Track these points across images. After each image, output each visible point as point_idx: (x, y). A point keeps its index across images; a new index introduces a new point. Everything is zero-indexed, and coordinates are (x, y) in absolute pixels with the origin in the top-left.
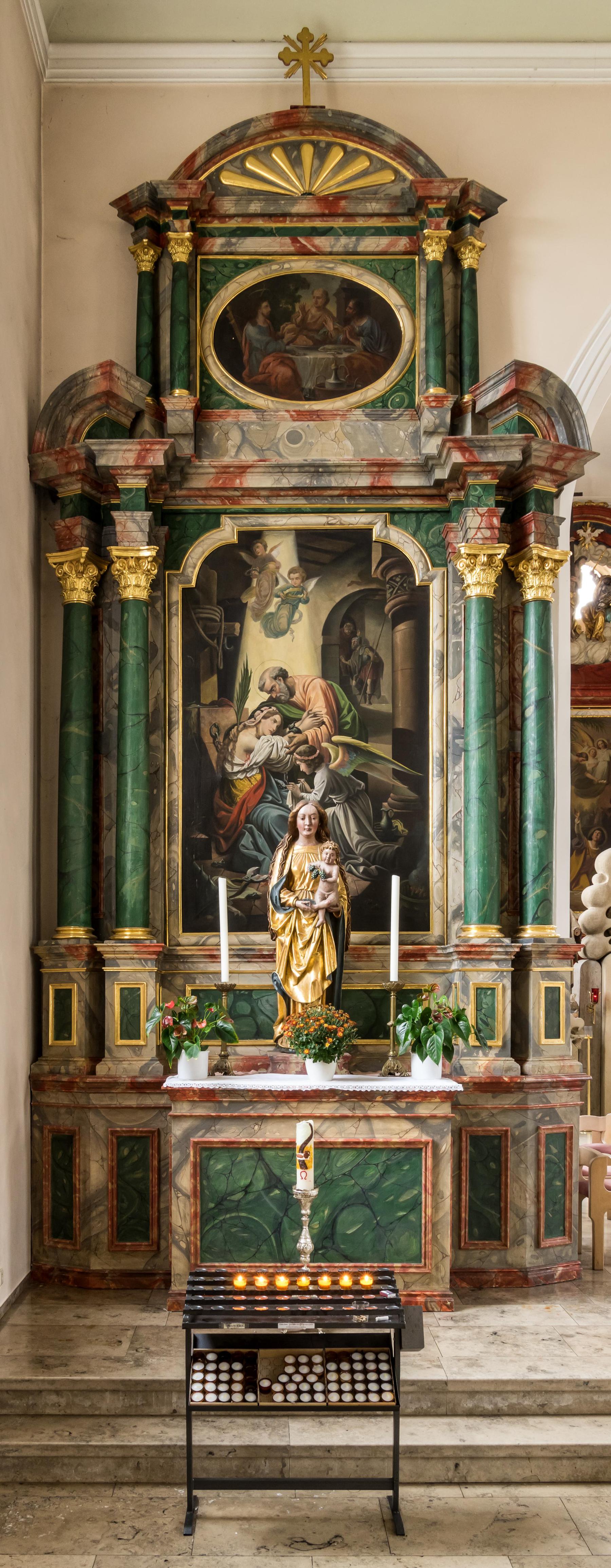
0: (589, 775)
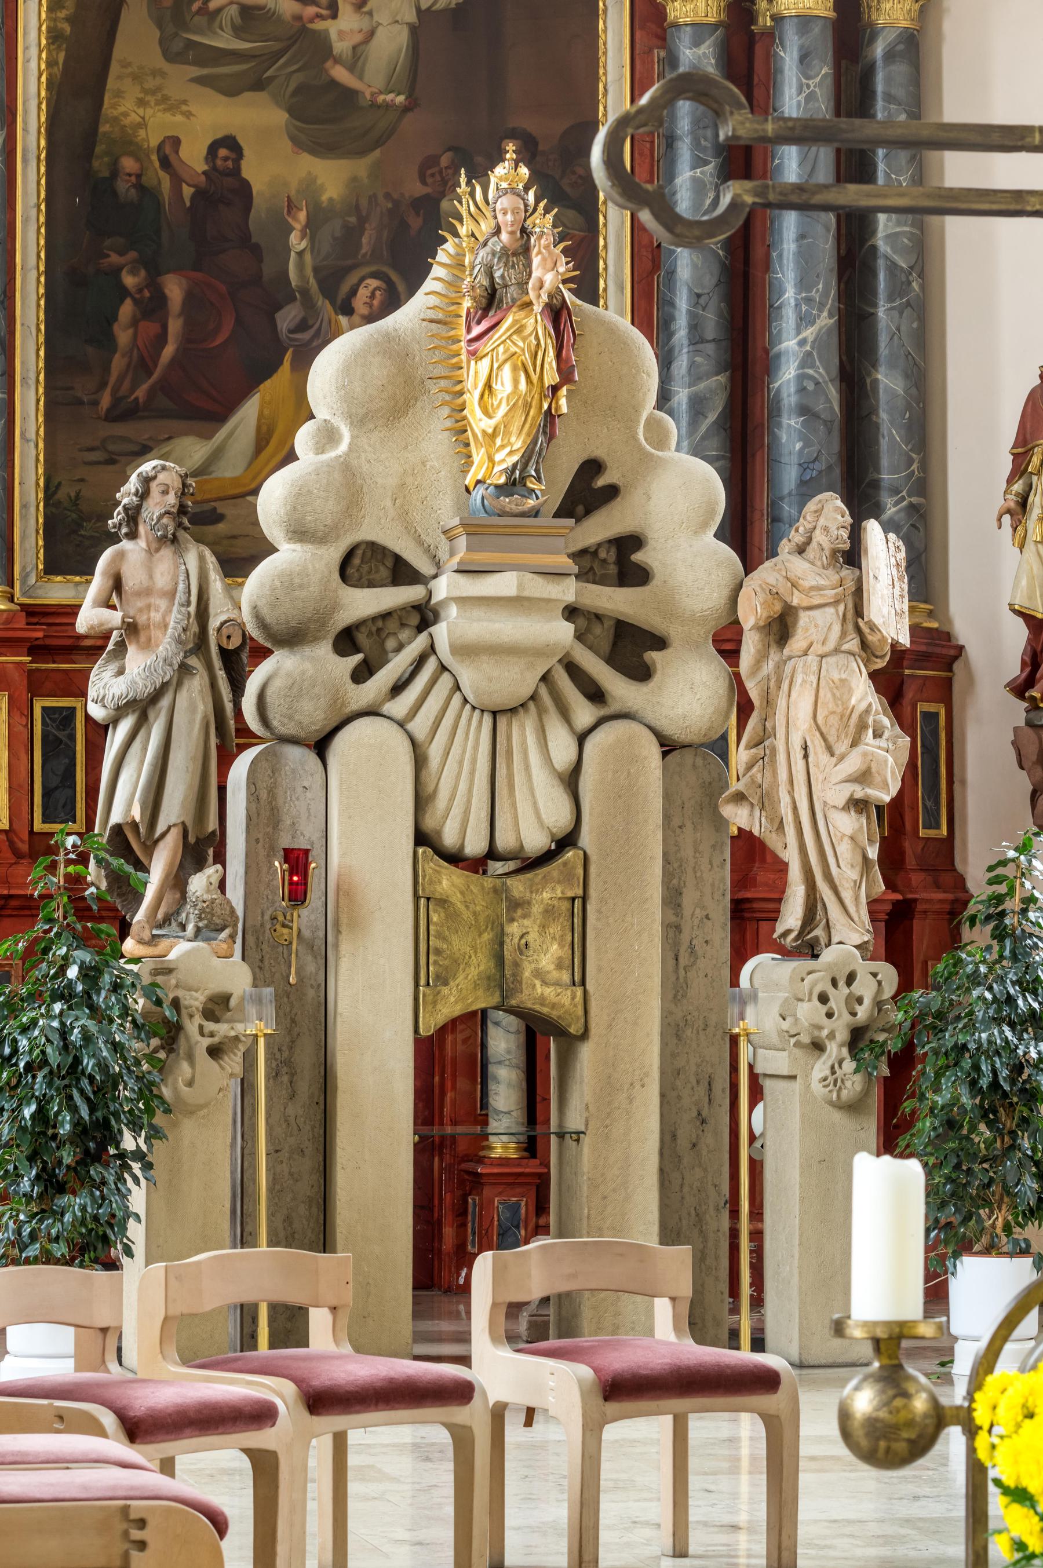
0: (340, 74)
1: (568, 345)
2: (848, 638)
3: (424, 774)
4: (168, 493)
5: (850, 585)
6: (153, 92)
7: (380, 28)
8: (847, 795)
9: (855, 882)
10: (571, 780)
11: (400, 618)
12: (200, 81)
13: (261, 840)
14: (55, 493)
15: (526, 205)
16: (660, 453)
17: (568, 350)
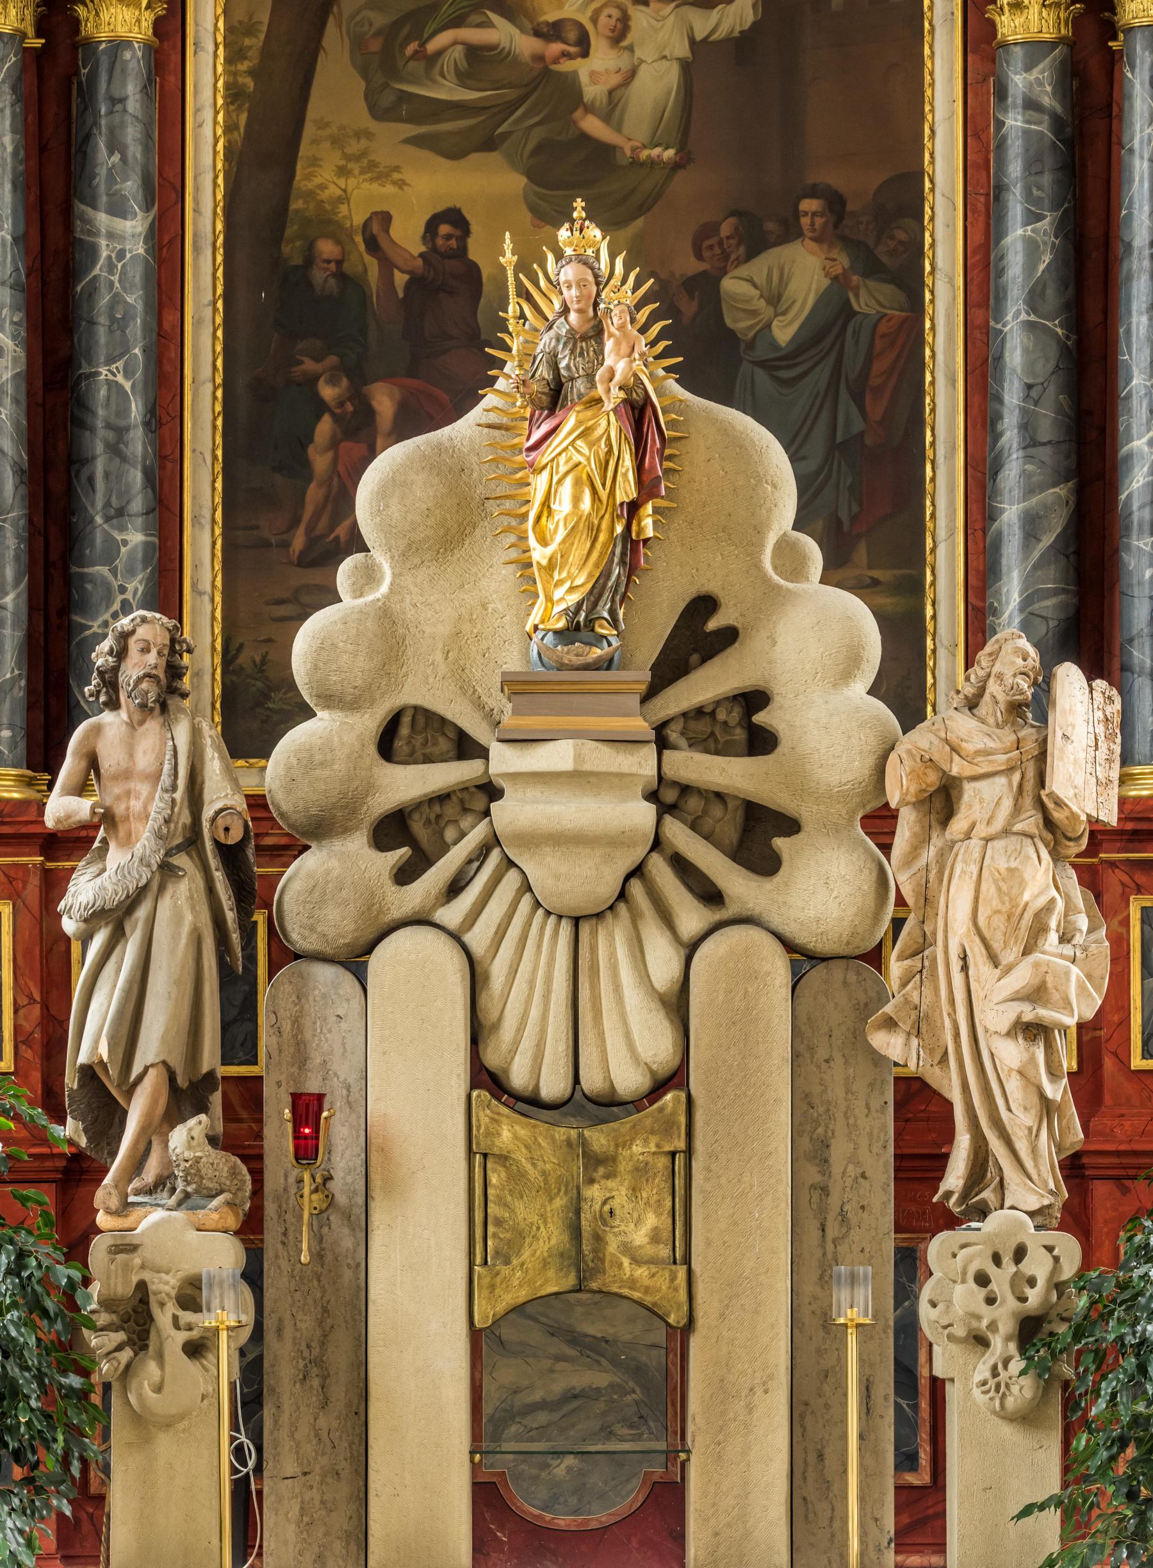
0: (593, 125)
1: (652, 452)
2: (1023, 816)
3: (483, 1000)
4: (149, 651)
5: (1031, 747)
6: (357, 158)
7: (643, 67)
9: (1030, 1129)
10: (677, 1005)
11: (462, 801)
12: (417, 141)
13: (284, 1083)
14: (235, 657)
15: (596, 276)
16: (790, 585)
17: (652, 458)
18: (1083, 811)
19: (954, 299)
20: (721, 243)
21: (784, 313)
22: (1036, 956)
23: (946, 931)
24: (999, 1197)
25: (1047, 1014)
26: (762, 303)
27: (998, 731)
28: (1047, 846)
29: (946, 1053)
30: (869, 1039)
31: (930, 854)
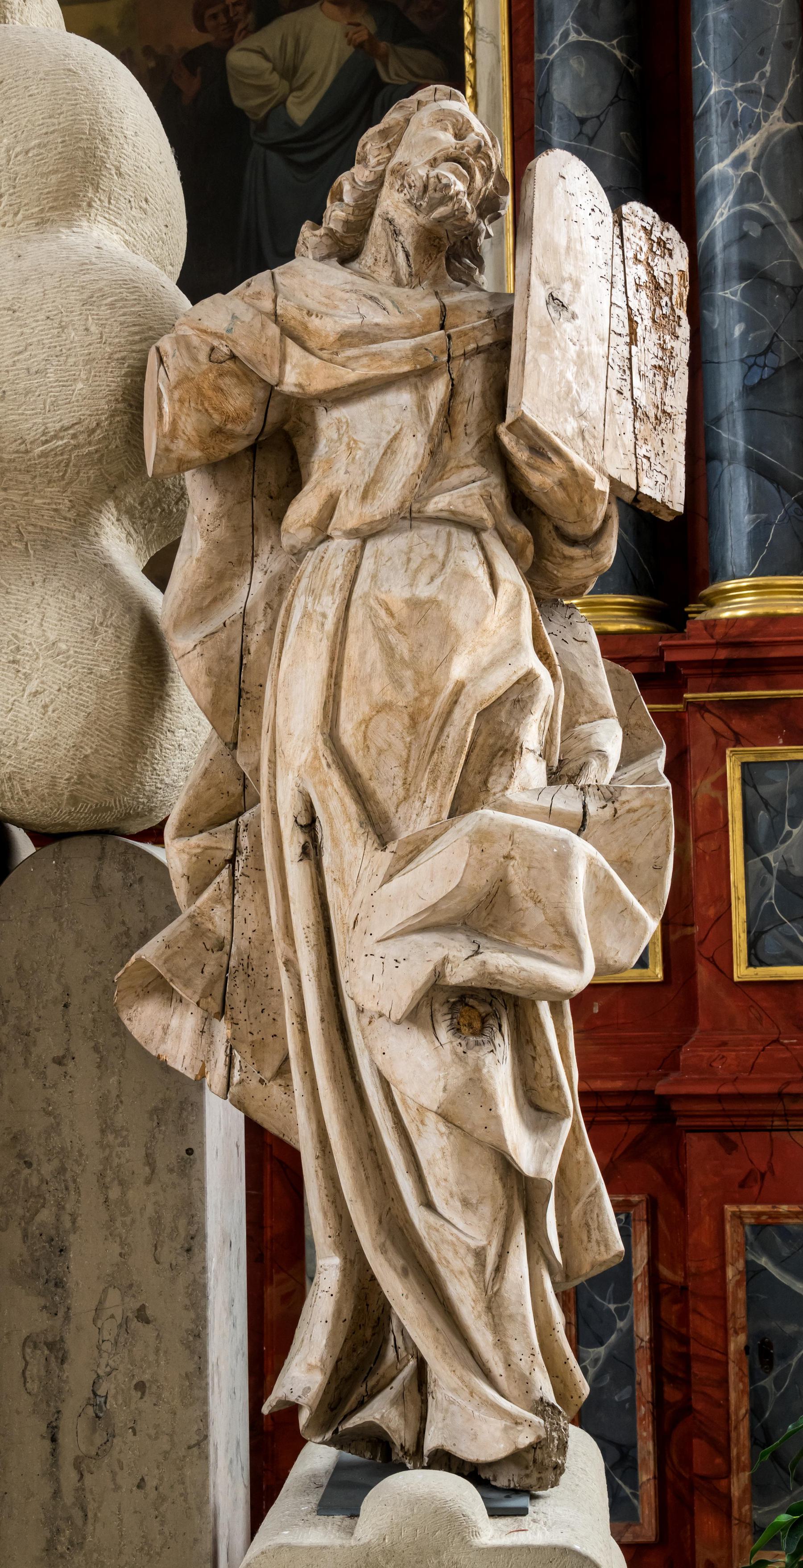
2: (454, 480)
8: (418, 974)
9: (479, 1255)
18: (601, 470)
19: (499, 60)
20: (226, 11)
21: (301, 88)
22: (486, 815)
23: (273, 763)
24: (413, 1416)
25: (507, 964)
26: (275, 77)
27: (394, 291)
28: (517, 556)
29: (286, 1059)
30: (124, 1017)
31: (252, 589)
